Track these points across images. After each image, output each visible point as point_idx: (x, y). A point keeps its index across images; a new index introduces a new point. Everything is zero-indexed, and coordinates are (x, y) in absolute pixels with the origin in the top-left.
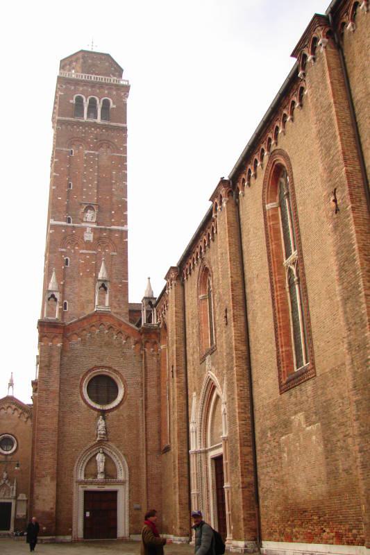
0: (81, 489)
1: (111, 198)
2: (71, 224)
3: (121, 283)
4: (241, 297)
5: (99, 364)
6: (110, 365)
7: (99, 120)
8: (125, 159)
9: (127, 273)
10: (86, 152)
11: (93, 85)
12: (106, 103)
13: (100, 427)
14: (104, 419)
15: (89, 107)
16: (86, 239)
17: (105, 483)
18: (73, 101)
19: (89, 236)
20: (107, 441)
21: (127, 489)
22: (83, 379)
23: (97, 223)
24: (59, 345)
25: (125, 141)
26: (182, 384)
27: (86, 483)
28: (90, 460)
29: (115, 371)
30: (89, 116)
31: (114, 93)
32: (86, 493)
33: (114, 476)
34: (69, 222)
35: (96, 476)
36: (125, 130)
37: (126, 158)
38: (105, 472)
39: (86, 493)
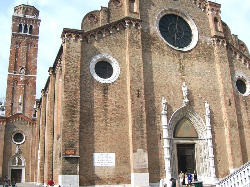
0: (11, 169)
1: (31, 64)
3: (33, 96)
4: (44, 122)
6: (21, 130)
7: (28, 34)
8: (37, 49)
11: (27, 19)
12: (31, 27)
13: (17, 150)
19: (22, 79)
21: (25, 168)
22: (12, 135)
23: (25, 74)
26: (38, 139)
29: (23, 132)
30: (24, 32)
32: (12, 170)
34: (15, 73)
36: (38, 38)
37: (37, 49)
39: (12, 170)
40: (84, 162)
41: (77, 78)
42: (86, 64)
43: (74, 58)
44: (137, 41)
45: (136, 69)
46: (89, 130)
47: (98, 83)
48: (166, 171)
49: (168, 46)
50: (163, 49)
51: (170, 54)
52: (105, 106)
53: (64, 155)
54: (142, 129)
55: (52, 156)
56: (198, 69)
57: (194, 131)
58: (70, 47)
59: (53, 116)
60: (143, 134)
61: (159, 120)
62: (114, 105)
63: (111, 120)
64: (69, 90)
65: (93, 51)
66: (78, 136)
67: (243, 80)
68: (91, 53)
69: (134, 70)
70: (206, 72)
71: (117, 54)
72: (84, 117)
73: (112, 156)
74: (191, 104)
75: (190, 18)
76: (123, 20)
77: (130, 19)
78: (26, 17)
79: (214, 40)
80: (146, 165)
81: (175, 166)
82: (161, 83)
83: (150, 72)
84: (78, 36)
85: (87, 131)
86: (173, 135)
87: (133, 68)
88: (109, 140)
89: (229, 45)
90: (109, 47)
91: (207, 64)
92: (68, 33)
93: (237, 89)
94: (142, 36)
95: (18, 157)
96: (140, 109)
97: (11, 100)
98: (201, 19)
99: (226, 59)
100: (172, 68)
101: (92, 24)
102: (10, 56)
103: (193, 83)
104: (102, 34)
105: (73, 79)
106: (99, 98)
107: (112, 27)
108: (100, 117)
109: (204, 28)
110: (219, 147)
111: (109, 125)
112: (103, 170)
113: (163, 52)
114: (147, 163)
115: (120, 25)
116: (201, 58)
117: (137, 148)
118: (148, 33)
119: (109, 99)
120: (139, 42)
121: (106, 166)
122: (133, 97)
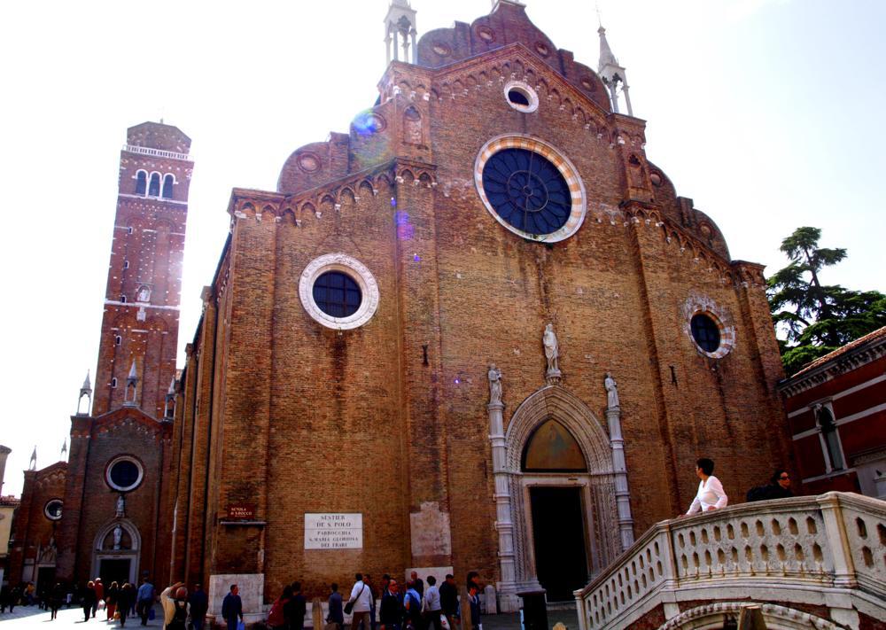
0: (98, 558)
2: (125, 304)
5: (122, 452)
6: (133, 452)
7: (160, 198)
9: (176, 352)
10: (145, 230)
12: (169, 179)
13: (119, 506)
14: (124, 499)
15: (152, 183)
16: (139, 318)
17: (121, 554)
18: (135, 177)
20: (126, 517)
21: (139, 557)
23: (150, 302)
24: (87, 437)
25: (184, 219)
27: (104, 553)
28: (109, 534)
30: (150, 194)
31: (178, 169)
32: (103, 562)
33: (130, 548)
35: (112, 547)
36: (185, 208)
37: (184, 237)
38: (121, 544)
39: (103, 562)
40: (278, 539)
41: (265, 317)
42: (289, 279)
43: (258, 265)
44: (423, 220)
45: (421, 292)
46: (293, 452)
47: (319, 330)
48: (502, 561)
49: (505, 230)
50: (493, 240)
51: (511, 253)
52: (339, 388)
53: (223, 519)
54: (435, 449)
55: (202, 522)
56: (585, 290)
57: (577, 453)
58: (248, 236)
59: (208, 415)
60: (436, 463)
61: (483, 423)
62: (363, 384)
63: (354, 424)
64: (242, 348)
65: (310, 246)
66: (264, 468)
67: (710, 315)
68: (303, 250)
69: (416, 295)
70: (607, 295)
71: (370, 253)
72: (283, 418)
73: (354, 522)
74: (570, 382)
75: (566, 158)
76: (392, 168)
77: (406, 163)
78: (157, 154)
79: (628, 213)
80: (446, 545)
81: (525, 549)
82: (486, 326)
83: (457, 298)
84: (269, 208)
85: (288, 456)
86: (519, 464)
87: (412, 288)
88: (346, 479)
89: (669, 225)
90: (351, 235)
91: (611, 275)
92: (241, 200)
93: (693, 340)
94: (436, 207)
95: (121, 528)
96: (430, 397)
97: (110, 372)
98: (594, 159)
99: (662, 260)
100: (517, 287)
101: (308, 178)
102: (112, 256)
103: (572, 326)
104: (333, 201)
105: (255, 320)
106: (323, 370)
107: (358, 183)
108: (324, 417)
109: (603, 182)
110: (647, 496)
111: (347, 437)
112: (330, 560)
113: (492, 247)
114: (447, 541)
115: (379, 178)
116: (595, 262)
117: (422, 501)
118: (454, 199)
119: (350, 369)
120: (427, 222)
121: (338, 550)
122: (410, 365)
